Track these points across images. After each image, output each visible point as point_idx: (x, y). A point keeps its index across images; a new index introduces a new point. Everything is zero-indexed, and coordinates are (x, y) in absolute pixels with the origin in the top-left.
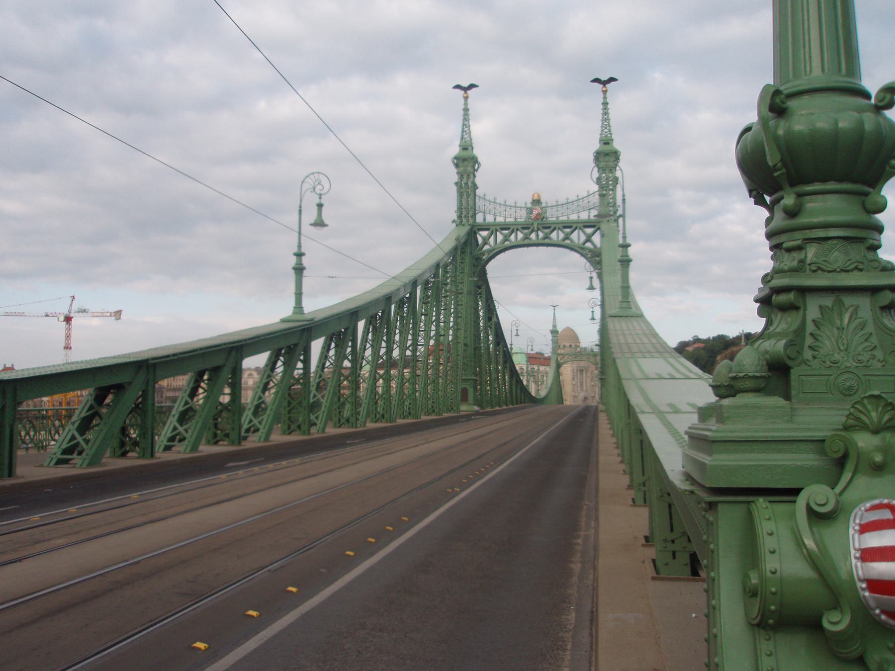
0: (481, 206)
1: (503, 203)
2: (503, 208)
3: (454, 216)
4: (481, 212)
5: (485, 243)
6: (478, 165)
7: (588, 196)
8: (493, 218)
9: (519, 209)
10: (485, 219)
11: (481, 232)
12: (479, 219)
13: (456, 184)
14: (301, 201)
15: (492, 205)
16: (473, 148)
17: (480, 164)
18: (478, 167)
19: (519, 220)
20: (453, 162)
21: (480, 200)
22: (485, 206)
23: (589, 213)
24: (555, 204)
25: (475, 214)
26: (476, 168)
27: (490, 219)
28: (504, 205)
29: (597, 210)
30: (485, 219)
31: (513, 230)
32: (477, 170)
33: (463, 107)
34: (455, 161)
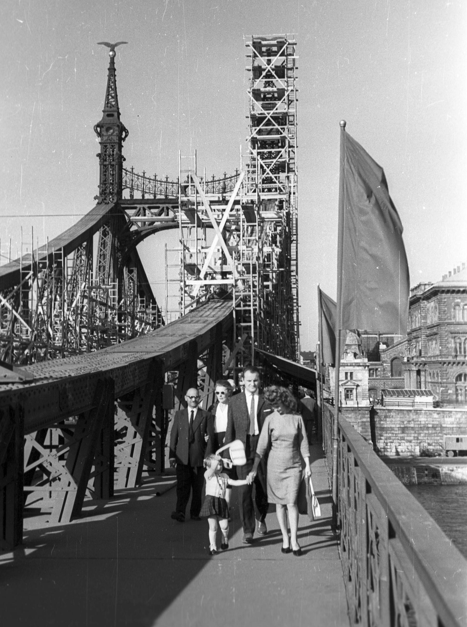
0: (128, 180)
1: (153, 178)
2: (152, 183)
3: (97, 192)
4: (128, 188)
6: (126, 133)
8: (141, 194)
9: (171, 184)
11: (127, 211)
12: (126, 194)
13: (99, 155)
15: (141, 180)
16: (119, 114)
17: (128, 132)
18: (126, 136)
19: (170, 197)
20: (96, 131)
21: (126, 174)
22: (132, 180)
26: (123, 136)
27: (138, 195)
28: (153, 180)
30: (132, 196)
31: (163, 208)
32: (124, 139)
33: (108, 66)
34: (99, 129)
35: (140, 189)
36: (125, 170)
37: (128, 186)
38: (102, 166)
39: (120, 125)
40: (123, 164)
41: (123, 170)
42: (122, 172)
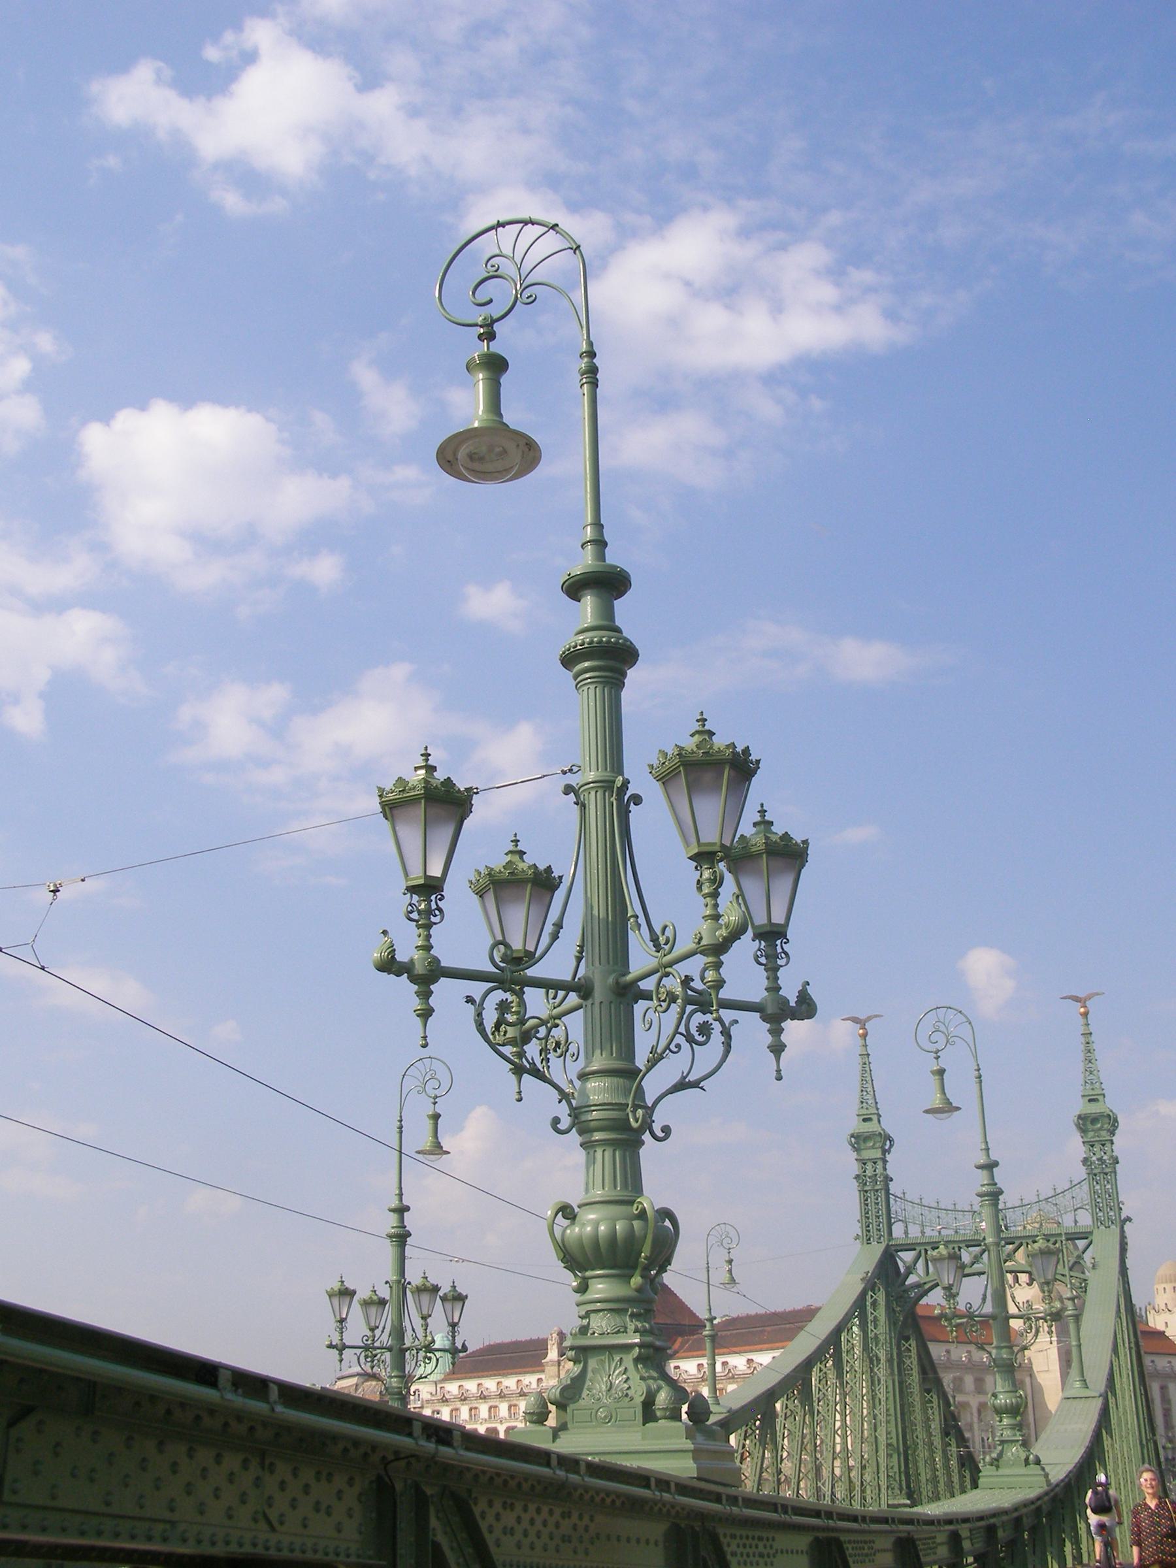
3: (857, 1229)
4: (900, 1220)
5: (910, 1270)
7: (1071, 1188)
10: (906, 1233)
12: (898, 1230)
13: (857, 1177)
14: (401, 1109)
15: (918, 1209)
19: (962, 1232)
22: (905, 1210)
23: (1075, 1216)
24: (1018, 1203)
25: (890, 1225)
27: (914, 1232)
28: (935, 1208)
29: (1087, 1210)
30: (906, 1233)
35: (917, 1222)
36: (893, 1195)
37: (901, 1218)
38: (862, 1193)
39: (882, 1132)
40: (890, 1186)
41: (891, 1196)
42: (889, 1197)
